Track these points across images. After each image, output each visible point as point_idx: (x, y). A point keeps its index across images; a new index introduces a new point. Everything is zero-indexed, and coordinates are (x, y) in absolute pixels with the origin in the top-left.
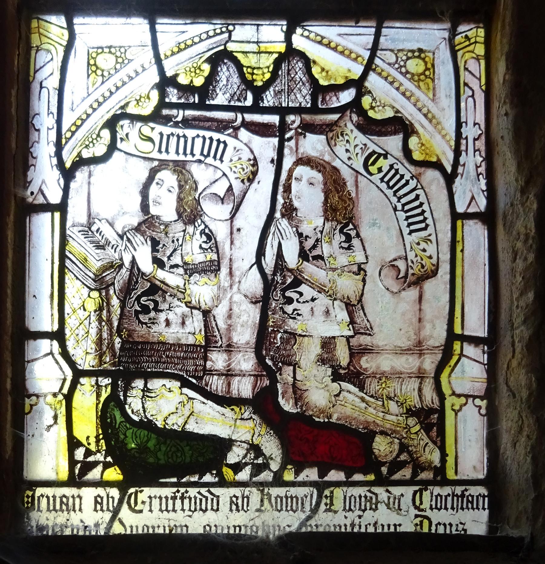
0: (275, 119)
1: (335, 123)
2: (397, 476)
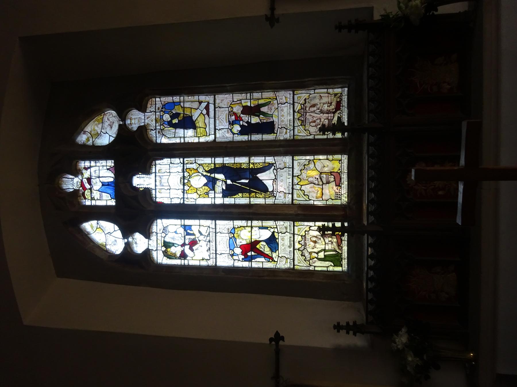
0: (305, 113)
1: (305, 107)
2: (341, 98)
